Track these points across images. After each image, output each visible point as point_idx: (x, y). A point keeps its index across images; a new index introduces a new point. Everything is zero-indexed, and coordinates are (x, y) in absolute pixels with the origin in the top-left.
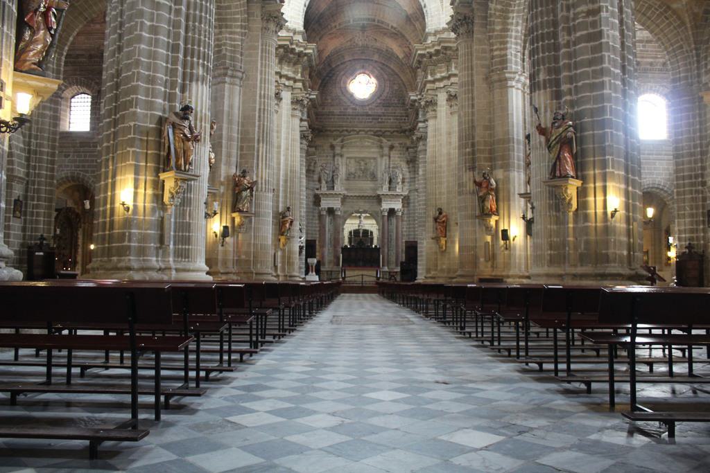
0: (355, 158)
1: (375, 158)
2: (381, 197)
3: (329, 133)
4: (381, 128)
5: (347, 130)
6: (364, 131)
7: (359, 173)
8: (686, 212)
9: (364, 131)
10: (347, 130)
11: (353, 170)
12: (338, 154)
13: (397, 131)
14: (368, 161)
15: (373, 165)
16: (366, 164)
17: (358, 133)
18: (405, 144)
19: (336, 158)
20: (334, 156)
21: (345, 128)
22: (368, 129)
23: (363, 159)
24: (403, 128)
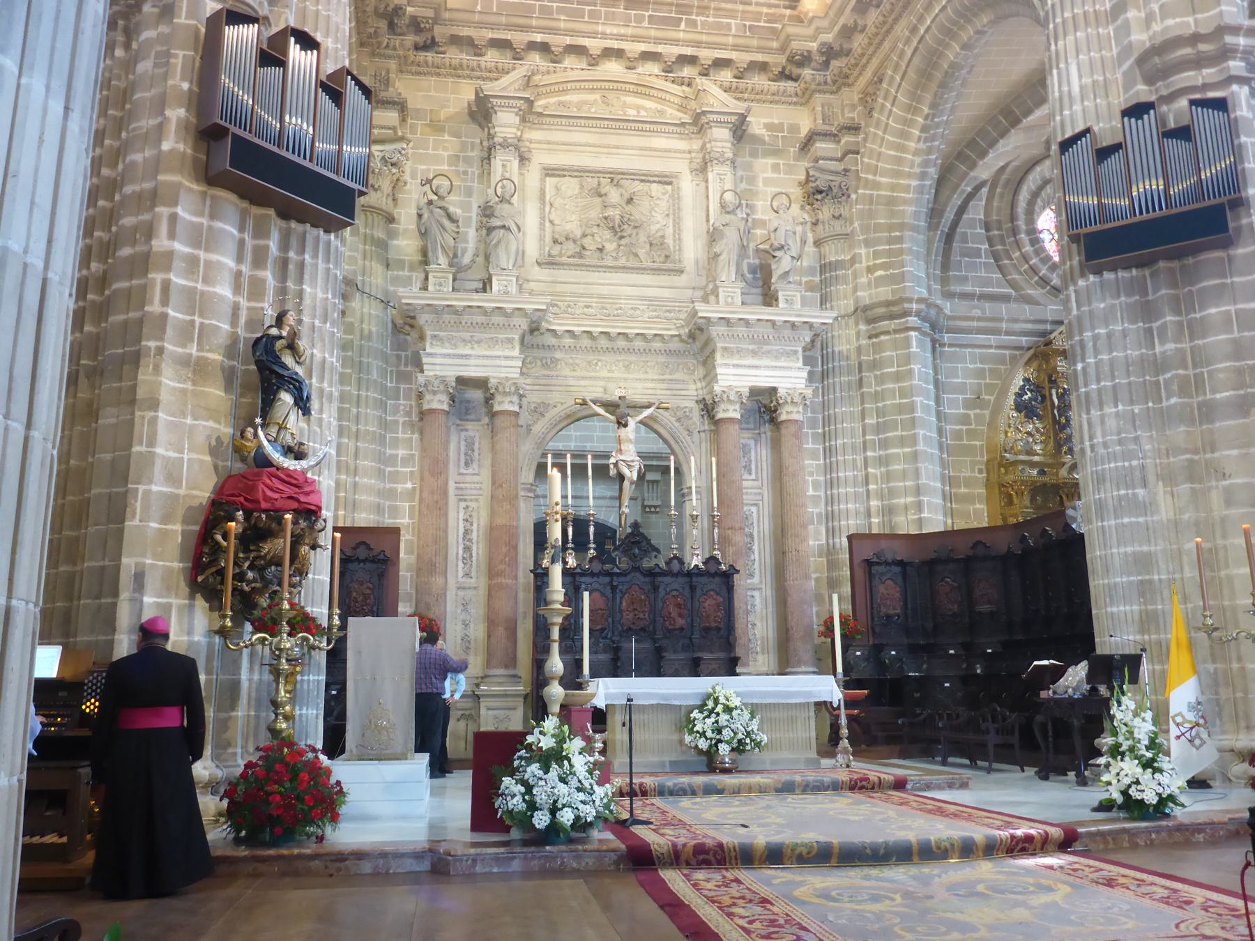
0: (579, 173)
1: (666, 180)
2: (716, 331)
3: (455, 55)
4: (698, 44)
5: (544, 48)
6: (619, 54)
7: (604, 236)
8: (1158, 548)
9: (619, 54)
10: (544, 48)
11: (572, 226)
12: (505, 145)
13: (763, 67)
14: (638, 187)
15: (663, 204)
16: (630, 201)
17: (594, 62)
18: (794, 129)
19: (497, 163)
20: (488, 158)
21: (539, 38)
22: (643, 47)
23: (615, 177)
24: (795, 45)
